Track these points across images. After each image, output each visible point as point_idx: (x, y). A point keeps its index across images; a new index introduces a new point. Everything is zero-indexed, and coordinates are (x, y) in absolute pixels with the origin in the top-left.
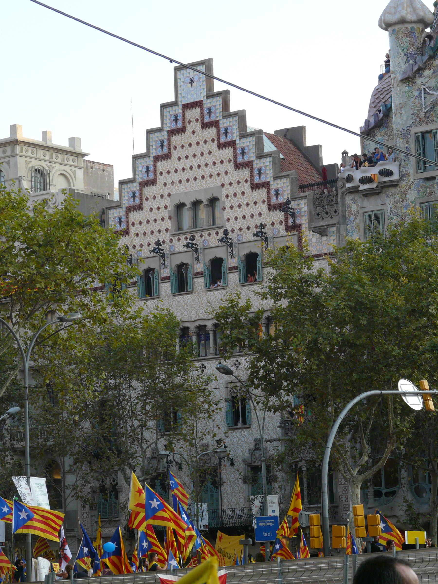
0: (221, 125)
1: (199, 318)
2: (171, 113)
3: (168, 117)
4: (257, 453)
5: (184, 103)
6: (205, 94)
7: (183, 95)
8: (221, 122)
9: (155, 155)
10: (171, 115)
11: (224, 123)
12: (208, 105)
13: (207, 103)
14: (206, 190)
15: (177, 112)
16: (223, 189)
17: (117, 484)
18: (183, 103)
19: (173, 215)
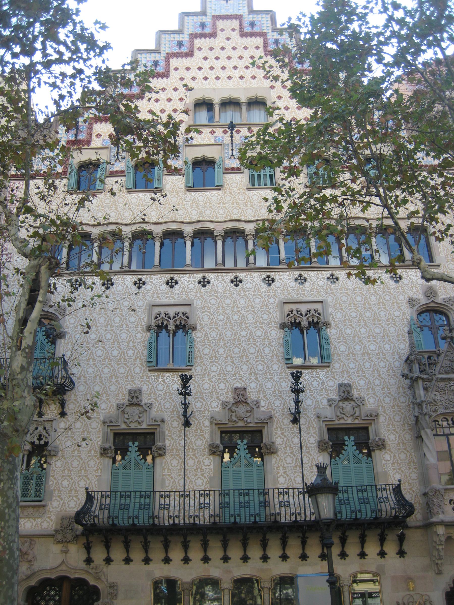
0: (268, 37)
1: (233, 218)
2: (195, 21)
3: (191, 24)
4: (348, 406)
5: (214, 13)
6: (246, 10)
7: (213, 8)
8: (268, 34)
9: (168, 51)
10: (195, 23)
11: (273, 36)
12: (251, 19)
13: (248, 18)
14: (245, 89)
15: (204, 20)
16: (272, 90)
17: (46, 444)
18: (213, 14)
19: (191, 107)
